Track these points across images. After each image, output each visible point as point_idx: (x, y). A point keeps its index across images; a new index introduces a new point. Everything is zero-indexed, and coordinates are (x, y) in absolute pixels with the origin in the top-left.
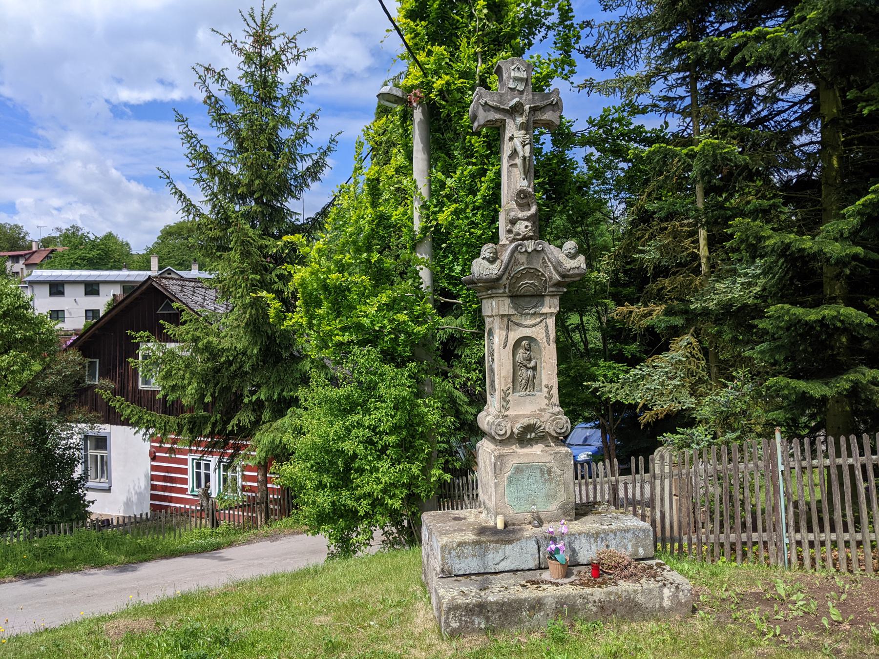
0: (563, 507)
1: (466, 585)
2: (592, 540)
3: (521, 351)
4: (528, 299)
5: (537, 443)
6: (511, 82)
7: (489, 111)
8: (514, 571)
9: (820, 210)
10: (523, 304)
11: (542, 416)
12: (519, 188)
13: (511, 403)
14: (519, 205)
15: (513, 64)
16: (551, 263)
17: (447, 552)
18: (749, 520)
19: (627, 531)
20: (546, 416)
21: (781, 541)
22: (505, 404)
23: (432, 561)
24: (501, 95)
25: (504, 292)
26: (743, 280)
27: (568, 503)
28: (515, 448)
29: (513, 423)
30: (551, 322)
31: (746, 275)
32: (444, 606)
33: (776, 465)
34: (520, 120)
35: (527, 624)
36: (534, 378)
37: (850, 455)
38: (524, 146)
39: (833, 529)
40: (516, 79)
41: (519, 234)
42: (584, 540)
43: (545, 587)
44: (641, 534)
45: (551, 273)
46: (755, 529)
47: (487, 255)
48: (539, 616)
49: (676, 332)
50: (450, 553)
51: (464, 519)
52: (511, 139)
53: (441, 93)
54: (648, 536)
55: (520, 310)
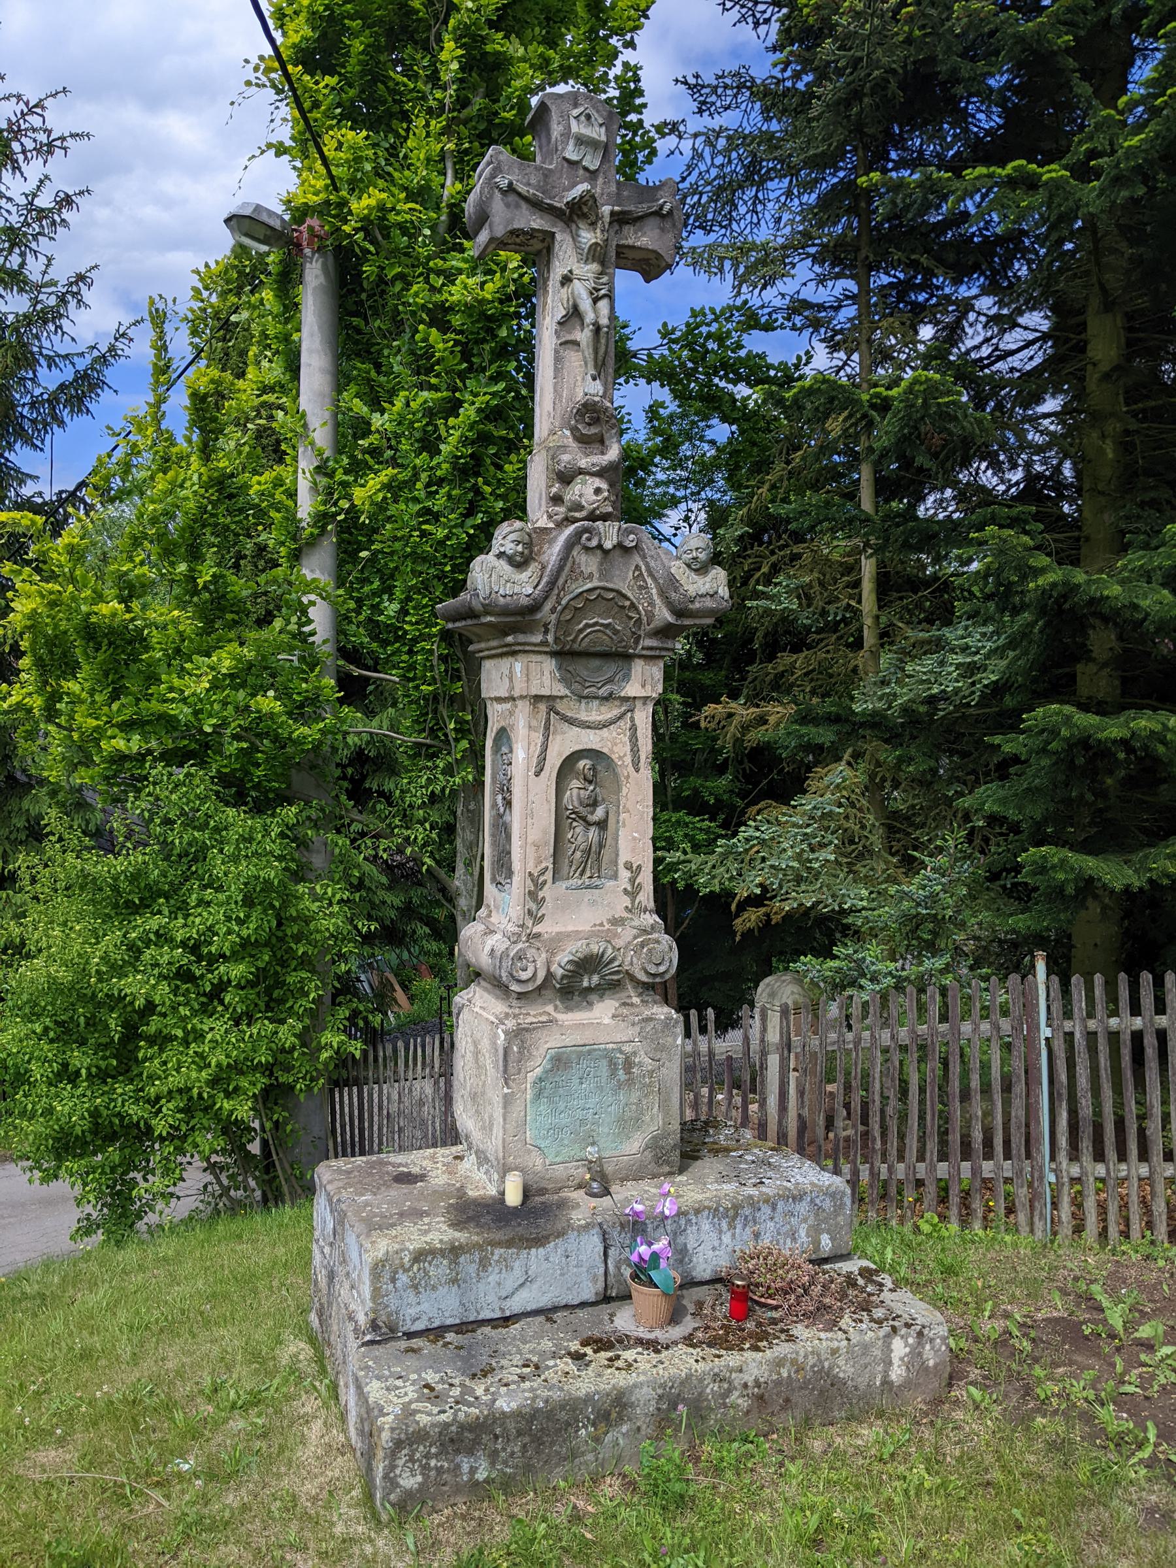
0: (654, 1145)
1: (435, 1366)
3: (575, 783)
4: (596, 663)
6: (571, 147)
7: (517, 206)
8: (547, 1313)
9: (1078, 539)
10: (584, 673)
11: (616, 935)
12: (579, 397)
13: (549, 904)
14: (583, 440)
15: (576, 106)
17: (387, 1276)
18: (977, 1136)
19: (798, 1197)
20: (626, 935)
21: (1041, 1178)
22: (534, 907)
23: (344, 1292)
24: (547, 174)
25: (544, 643)
26: (960, 659)
27: (665, 1135)
29: (552, 953)
30: (643, 718)
31: (965, 649)
32: (385, 1435)
33: (1034, 1027)
34: (588, 237)
35: (590, 1457)
36: (601, 846)
38: (595, 301)
39: (1144, 1156)
40: (581, 141)
41: (579, 507)
42: (706, 1226)
43: (629, 1355)
44: (828, 1204)
47: (509, 548)
48: (619, 1435)
49: (825, 755)
50: (393, 1280)
51: (422, 1177)
52: (567, 280)
53: (367, 225)
54: (842, 1205)
55: (576, 686)
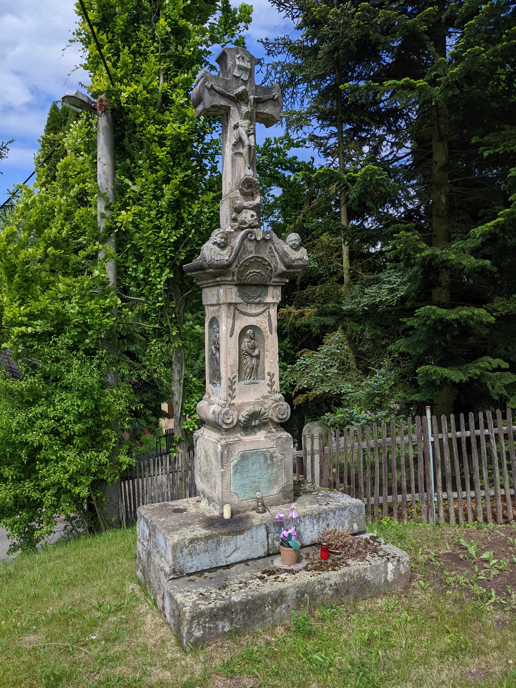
0: (283, 491)
1: (202, 585)
2: (315, 521)
3: (246, 340)
4: (254, 288)
5: (260, 430)
6: (236, 70)
7: (215, 96)
8: (245, 562)
9: (431, 236)
10: (249, 293)
11: (265, 403)
12: (242, 176)
13: (237, 391)
14: (244, 194)
15: (238, 53)
16: (278, 253)
17: (179, 550)
18: (404, 484)
19: (344, 509)
20: (269, 403)
21: (431, 499)
22: (231, 392)
23: (157, 560)
24: (227, 82)
25: (233, 280)
26: (388, 286)
27: (287, 486)
28: (238, 435)
29: (239, 412)
30: (273, 311)
31: (389, 282)
32: (187, 615)
33: (426, 437)
34: (245, 109)
35: (270, 619)
36: (258, 366)
37: (486, 427)
38: (249, 135)
39: (472, 488)
40: (240, 68)
41: (244, 223)
42: (308, 522)
43: (283, 576)
44: (356, 511)
45: (277, 263)
46: (409, 490)
47: (218, 240)
48: (281, 609)
50: (182, 552)
51: (185, 510)
52: (236, 127)
53: (129, 100)
54: (361, 512)
55: (246, 299)
